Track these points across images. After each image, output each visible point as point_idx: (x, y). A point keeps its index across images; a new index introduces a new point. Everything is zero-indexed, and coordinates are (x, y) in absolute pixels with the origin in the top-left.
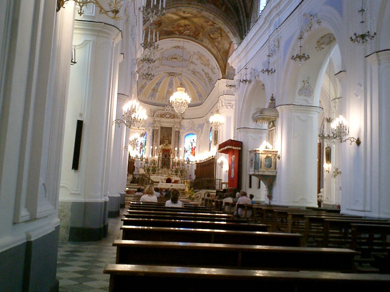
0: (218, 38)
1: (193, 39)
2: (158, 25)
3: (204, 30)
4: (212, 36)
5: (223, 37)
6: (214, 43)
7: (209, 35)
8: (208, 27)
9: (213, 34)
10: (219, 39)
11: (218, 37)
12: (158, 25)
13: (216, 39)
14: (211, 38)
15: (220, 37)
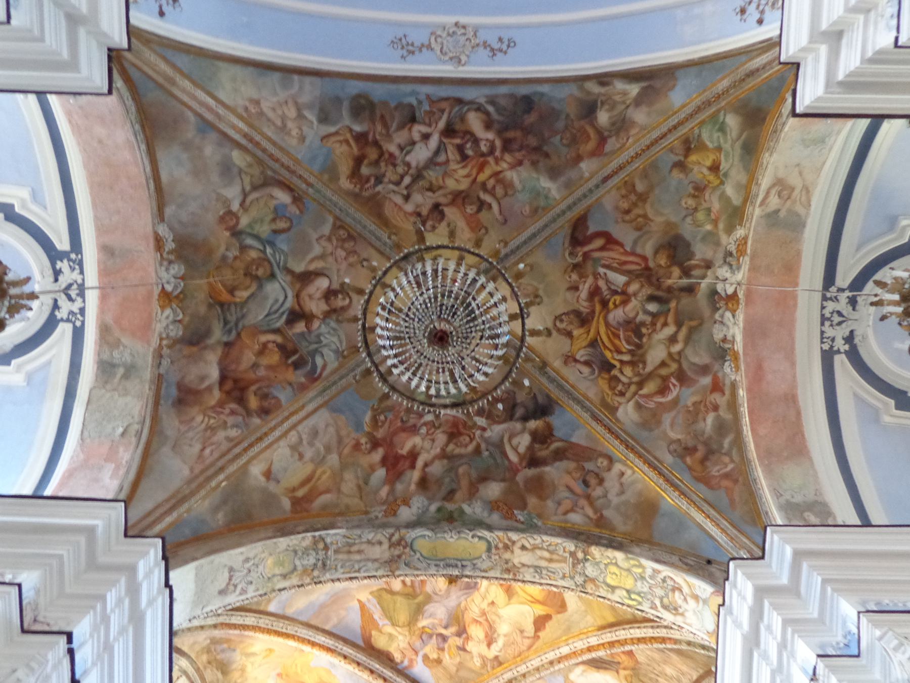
0: (245, 195)
1: (378, 92)
2: (592, 228)
3: (339, 225)
4: (283, 197)
5: (222, 219)
6: (260, 162)
7: (297, 200)
8: (317, 250)
9: (278, 213)
10: (233, 193)
11: (242, 204)
12: (592, 228)
13: (255, 188)
14: (287, 187)
15: (235, 206)
